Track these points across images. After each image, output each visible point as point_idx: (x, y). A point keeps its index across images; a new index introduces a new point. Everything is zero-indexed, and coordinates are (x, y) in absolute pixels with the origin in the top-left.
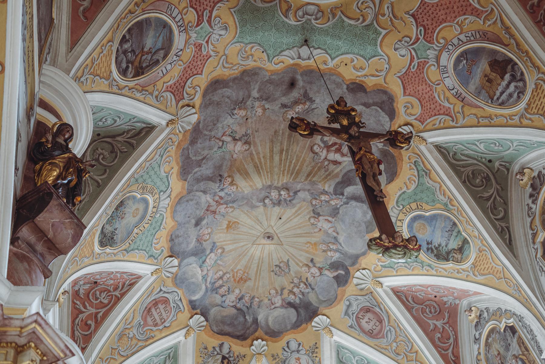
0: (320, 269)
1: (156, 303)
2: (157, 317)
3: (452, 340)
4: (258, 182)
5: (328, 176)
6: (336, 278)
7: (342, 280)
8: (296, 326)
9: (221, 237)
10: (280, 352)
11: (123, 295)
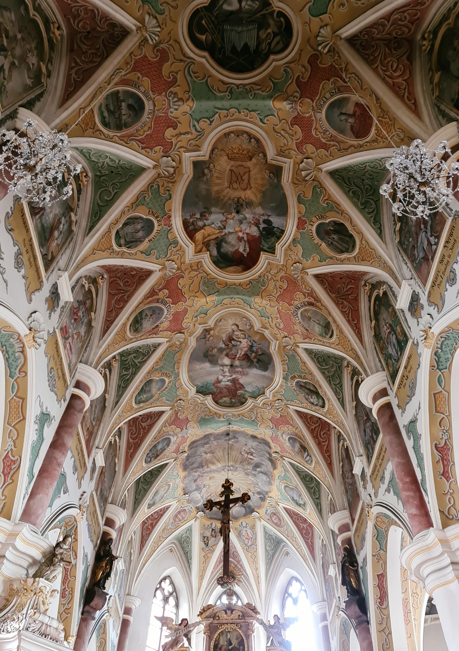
0: (253, 493)
1: (179, 512)
2: (180, 517)
3: (310, 535)
4: (219, 465)
5: (249, 464)
6: (260, 498)
7: (263, 499)
8: (245, 515)
9: (207, 482)
10: (238, 527)
11: (164, 513)
